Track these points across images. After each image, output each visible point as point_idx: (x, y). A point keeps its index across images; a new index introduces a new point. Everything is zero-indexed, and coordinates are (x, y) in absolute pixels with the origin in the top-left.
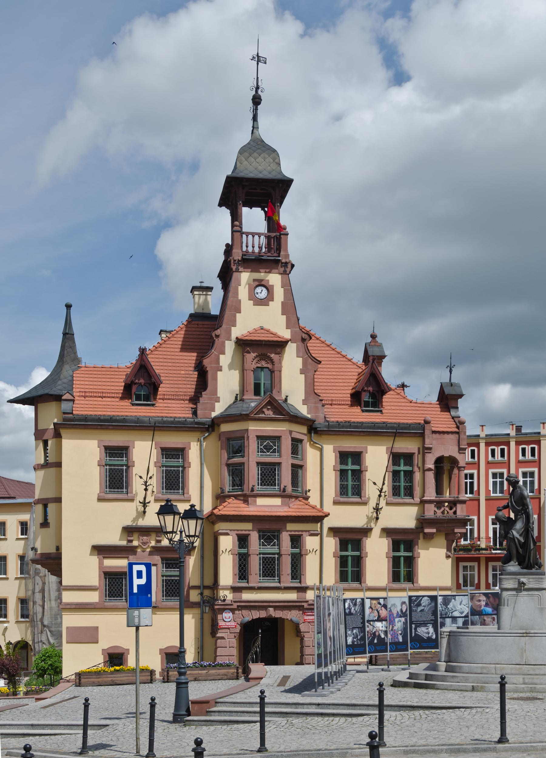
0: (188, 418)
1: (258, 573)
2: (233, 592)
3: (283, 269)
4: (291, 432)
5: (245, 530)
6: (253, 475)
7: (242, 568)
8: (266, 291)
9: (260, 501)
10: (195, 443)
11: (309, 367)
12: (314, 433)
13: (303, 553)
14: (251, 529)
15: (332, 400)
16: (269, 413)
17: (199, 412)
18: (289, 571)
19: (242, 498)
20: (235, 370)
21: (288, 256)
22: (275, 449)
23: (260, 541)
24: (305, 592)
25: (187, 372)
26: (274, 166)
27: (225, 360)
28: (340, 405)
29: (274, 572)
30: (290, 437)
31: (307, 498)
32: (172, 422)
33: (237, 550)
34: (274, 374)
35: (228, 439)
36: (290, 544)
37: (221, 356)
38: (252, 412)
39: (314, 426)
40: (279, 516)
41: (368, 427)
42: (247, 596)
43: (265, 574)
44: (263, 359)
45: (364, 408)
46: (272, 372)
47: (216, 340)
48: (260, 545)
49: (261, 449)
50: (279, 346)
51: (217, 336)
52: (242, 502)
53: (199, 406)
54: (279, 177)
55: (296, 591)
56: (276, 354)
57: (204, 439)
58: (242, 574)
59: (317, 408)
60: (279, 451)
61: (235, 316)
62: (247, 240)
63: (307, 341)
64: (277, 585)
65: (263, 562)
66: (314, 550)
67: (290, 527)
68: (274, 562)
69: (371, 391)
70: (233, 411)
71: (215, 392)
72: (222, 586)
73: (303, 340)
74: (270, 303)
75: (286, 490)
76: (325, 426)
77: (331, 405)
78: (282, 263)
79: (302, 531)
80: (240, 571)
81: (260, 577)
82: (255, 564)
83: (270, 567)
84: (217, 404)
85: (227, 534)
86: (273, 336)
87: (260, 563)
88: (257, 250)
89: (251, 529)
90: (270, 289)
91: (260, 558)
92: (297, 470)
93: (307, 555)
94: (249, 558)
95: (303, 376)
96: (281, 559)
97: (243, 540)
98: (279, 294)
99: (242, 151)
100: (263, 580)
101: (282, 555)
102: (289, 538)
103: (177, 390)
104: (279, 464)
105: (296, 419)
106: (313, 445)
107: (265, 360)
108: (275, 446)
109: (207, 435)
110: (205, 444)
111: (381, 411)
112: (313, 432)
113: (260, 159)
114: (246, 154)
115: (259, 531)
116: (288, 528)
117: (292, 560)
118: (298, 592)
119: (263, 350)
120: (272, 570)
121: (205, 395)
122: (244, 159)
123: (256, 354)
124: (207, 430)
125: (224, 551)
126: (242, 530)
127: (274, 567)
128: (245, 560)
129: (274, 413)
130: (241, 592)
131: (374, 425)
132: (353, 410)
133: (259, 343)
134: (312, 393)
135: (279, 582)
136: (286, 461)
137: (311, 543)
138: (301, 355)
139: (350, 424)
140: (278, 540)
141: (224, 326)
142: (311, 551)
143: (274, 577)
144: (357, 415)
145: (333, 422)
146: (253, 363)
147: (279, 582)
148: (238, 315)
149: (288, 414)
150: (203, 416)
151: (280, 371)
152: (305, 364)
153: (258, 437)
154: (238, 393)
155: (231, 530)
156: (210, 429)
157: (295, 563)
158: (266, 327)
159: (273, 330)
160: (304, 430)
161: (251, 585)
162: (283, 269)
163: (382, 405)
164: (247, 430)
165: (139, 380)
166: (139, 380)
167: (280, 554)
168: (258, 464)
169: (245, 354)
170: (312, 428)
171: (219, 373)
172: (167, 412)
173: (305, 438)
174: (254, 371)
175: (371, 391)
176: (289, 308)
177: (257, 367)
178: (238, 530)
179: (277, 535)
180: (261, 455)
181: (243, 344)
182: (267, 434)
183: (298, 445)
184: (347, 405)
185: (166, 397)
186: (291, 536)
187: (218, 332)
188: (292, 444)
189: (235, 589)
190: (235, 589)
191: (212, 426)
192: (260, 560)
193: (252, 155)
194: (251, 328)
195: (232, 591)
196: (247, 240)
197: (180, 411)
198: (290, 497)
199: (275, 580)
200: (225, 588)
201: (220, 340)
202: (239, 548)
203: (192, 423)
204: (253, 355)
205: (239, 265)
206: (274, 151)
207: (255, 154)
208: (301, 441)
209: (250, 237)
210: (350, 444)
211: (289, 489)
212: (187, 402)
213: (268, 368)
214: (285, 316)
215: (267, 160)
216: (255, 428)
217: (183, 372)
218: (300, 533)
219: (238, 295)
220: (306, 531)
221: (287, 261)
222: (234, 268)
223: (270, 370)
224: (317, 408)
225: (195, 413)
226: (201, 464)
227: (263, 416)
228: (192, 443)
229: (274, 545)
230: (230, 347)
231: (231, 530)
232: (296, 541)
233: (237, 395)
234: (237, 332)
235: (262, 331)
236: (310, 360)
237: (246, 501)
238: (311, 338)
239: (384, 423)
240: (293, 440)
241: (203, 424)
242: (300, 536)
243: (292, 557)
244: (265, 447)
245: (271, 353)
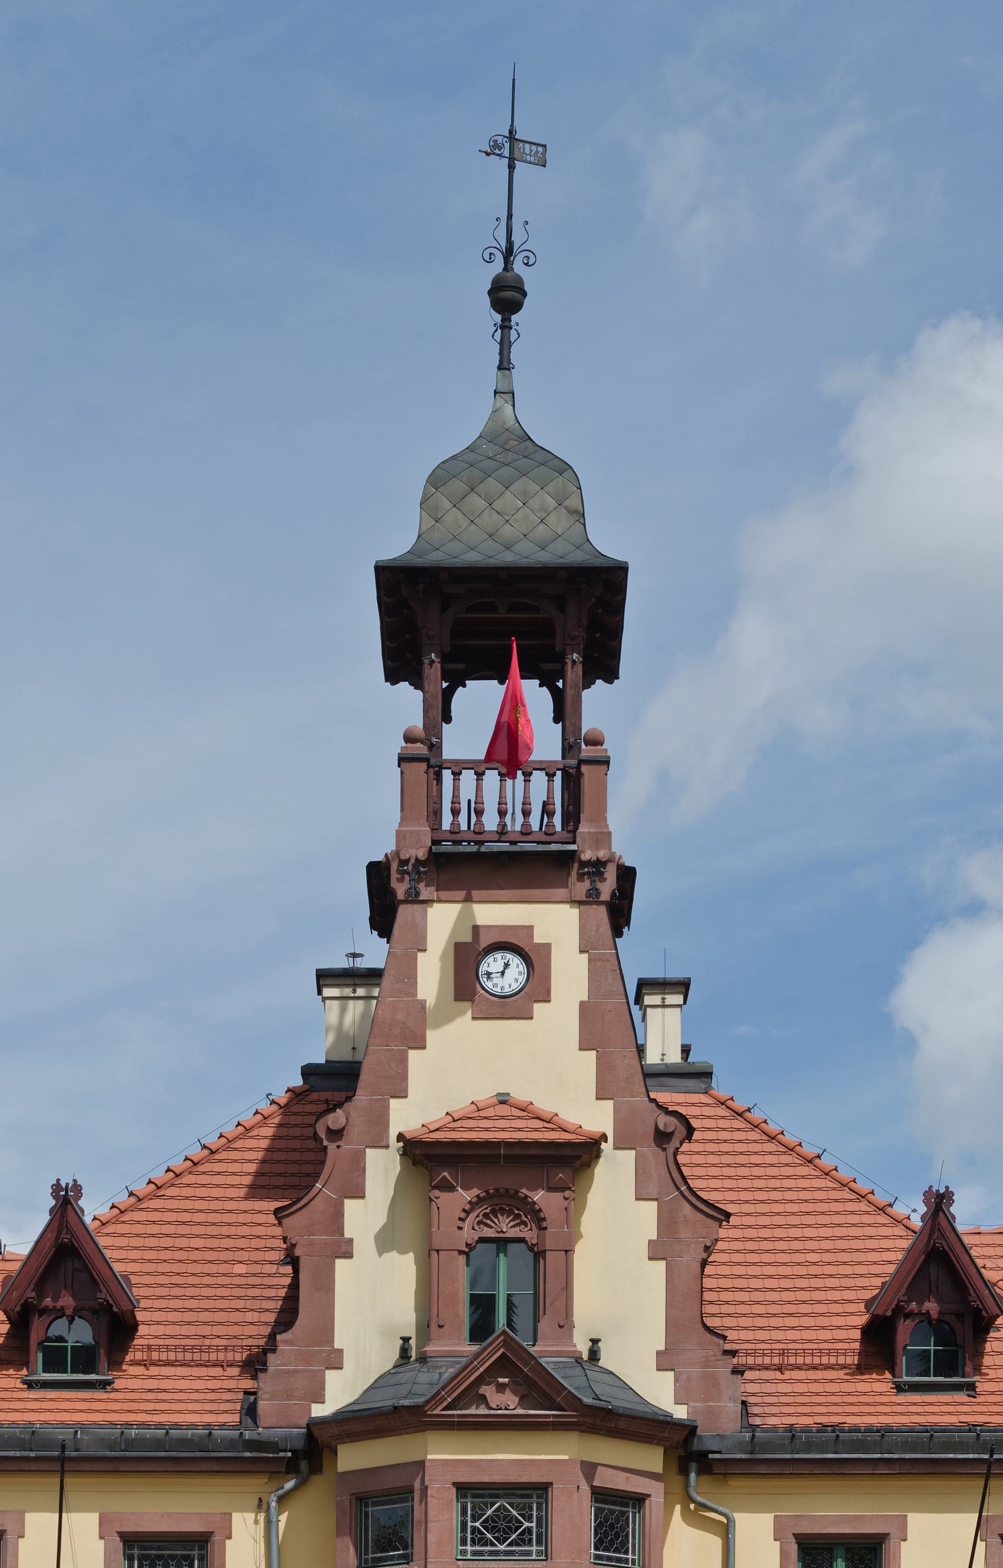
0: (223, 1426)
3: (587, 884)
4: (589, 1469)
8: (523, 968)
11: (685, 1233)
12: (700, 1473)
15: (783, 1353)
16: (504, 1401)
17: (263, 1405)
20: (402, 1252)
21: (604, 838)
22: (529, 1530)
25: (256, 1269)
26: (559, 522)
27: (364, 1218)
28: (814, 1368)
30: (585, 1488)
32: (159, 1444)
34: (546, 1262)
35: (362, 1500)
37: (351, 1206)
38: (435, 1399)
41: (905, 1446)
44: (503, 1211)
45: (905, 1379)
46: (539, 1255)
47: (332, 1147)
49: (474, 1529)
50: (570, 1159)
51: (336, 1134)
53: (266, 1384)
54: (577, 557)
56: (551, 1189)
59: (711, 1382)
61: (404, 1061)
62: (456, 789)
63: (675, 1142)
69: (934, 1314)
70: (384, 1401)
71: (326, 1330)
73: (662, 1137)
74: (538, 1008)
76: (740, 1446)
77: (780, 1369)
78: (583, 864)
84: (330, 1375)
86: (539, 1124)
88: (491, 822)
90: (534, 958)
95: (661, 1266)
98: (571, 975)
99: (437, 480)
103: (205, 1330)
106: (696, 1517)
107: (510, 1212)
108: (529, 1519)
111: (971, 1387)
112: (693, 1466)
113: (509, 500)
114: (458, 486)
119: (506, 1178)
122: (447, 504)
123: (475, 1191)
124: (291, 1467)
129: (524, 1401)
131: (930, 1436)
132: (863, 1387)
133: (484, 1152)
134: (694, 1329)
138: (653, 1190)
139: (835, 1435)
141: (362, 1097)
144: (877, 1404)
145: (774, 1428)
146: (467, 1225)
148: (413, 1055)
149: (574, 1402)
150: (279, 1420)
151: (568, 1252)
152: (666, 1223)
153: (462, 1489)
154: (411, 1332)
156: (304, 1465)
158: (520, 1094)
159: (544, 1104)
162: (587, 884)
163: (977, 1369)
164: (421, 1464)
165: (55, 1299)
166: (55, 1299)
169: (436, 1193)
170: (689, 1454)
171: (340, 1263)
172: (150, 1406)
173: (655, 1490)
174: (468, 1252)
175: (934, 1314)
176: (608, 1027)
177: (482, 1240)
180: (475, 1553)
181: (430, 1159)
182: (498, 1478)
183: (624, 1514)
184: (844, 1367)
185: (155, 1356)
187: (336, 1119)
188: (598, 1512)
191: (310, 1452)
193: (480, 488)
194: (459, 1103)
196: (456, 789)
197: (192, 1400)
201: (346, 1145)
203: (231, 1444)
204: (465, 1196)
205: (419, 876)
206: (564, 468)
207: (492, 484)
208: (639, 1500)
209: (468, 777)
210: (840, 1510)
212: (235, 1371)
213: (522, 1240)
214: (593, 1054)
215: (535, 503)
217: (240, 1269)
219: (415, 984)
221: (602, 854)
222: (401, 890)
223: (531, 1248)
224: (711, 1382)
225: (251, 1411)
227: (483, 1411)
228: (237, 1518)
230: (382, 1169)
233: (406, 1340)
234: (408, 1116)
235: (504, 1110)
236: (687, 1207)
238: (690, 1130)
239: (972, 1427)
241: (271, 1446)
244: (491, 1524)
245: (534, 1188)
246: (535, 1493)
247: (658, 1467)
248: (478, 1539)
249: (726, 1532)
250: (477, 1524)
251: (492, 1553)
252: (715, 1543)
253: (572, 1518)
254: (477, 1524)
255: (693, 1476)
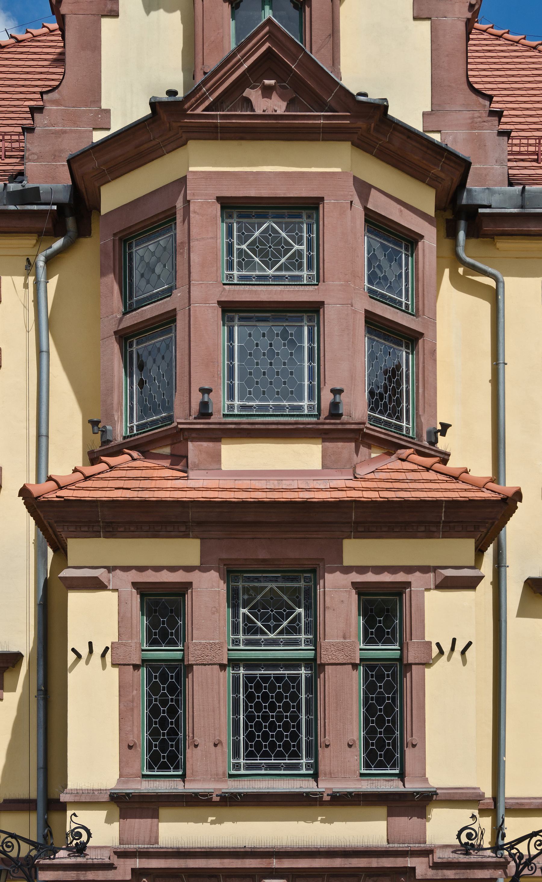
1: (227, 738)
2: (123, 816)
5: (173, 569)
6: (208, 356)
7: (163, 723)
9: (237, 456)
10: (19, 280)
13: (412, 657)
14: (196, 562)
18: (356, 731)
19: (167, 450)
23: (235, 615)
24: (423, 815)
29: (295, 736)
31: (444, 458)
33: (138, 647)
36: (357, 623)
39: (464, 200)
40: (306, 505)
42: (175, 832)
43: (258, 746)
48: (235, 630)
52: (167, 463)
55: (383, 811)
57: (49, 260)
58: (163, 745)
60: (316, 263)
64: (307, 786)
65: (250, 697)
66: (459, 647)
67: (357, 551)
68: (295, 697)
72: (77, 792)
75: (343, 409)
79: (409, 570)
80: (153, 733)
81: (236, 754)
82: (212, 706)
83: (279, 718)
85: (95, 585)
87: (236, 702)
89: (196, 562)
91: (236, 680)
92: (398, 338)
93: (427, 664)
94: (189, 681)
96: (320, 682)
97: (162, 609)
100: (248, 767)
101: (323, 666)
102: (354, 597)
104: (314, 309)
105: (369, 126)
108: (300, 243)
109: (58, 244)
110: (53, 282)
115: (230, 573)
116: (347, 561)
117: (370, 688)
118: (391, 814)
120: (286, 726)
121: (56, 102)
125: (84, 652)
126: (157, 569)
127: (295, 718)
128: (173, 689)
130: (155, 815)
135: (315, 776)
136: (345, 299)
137: (446, 616)
140: (311, 607)
142: (446, 648)
143: (296, 755)
147: (315, 776)
155: (110, 569)
156: (70, 222)
157: (380, 700)
160: (426, 199)
161: (193, 786)
167: (315, 666)
168: (230, 310)
178: (141, 569)
179: (308, 592)
180: (241, 277)
186: (361, 589)
189: (126, 805)
190: (126, 805)
192: (236, 690)
195: (116, 811)
198: (359, 437)
199: (297, 767)
200: (89, 802)
202: (152, 641)
208: (411, 240)
211: (357, 408)
216: (210, 168)
218: (400, 577)
220: (425, 569)
226: (41, 352)
229: (293, 629)
231: (110, 569)
232: (384, 610)
237: (179, 460)
240: (375, 223)
242: (399, 590)
243: (366, 676)
246: (308, 207)
247: (430, 210)
248: (245, 262)
249: (494, 297)
250: (244, 247)
251: (259, 277)
252: (485, 307)
253: (344, 235)
254: (244, 247)
255: (462, 235)
